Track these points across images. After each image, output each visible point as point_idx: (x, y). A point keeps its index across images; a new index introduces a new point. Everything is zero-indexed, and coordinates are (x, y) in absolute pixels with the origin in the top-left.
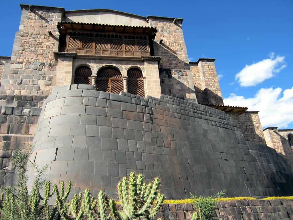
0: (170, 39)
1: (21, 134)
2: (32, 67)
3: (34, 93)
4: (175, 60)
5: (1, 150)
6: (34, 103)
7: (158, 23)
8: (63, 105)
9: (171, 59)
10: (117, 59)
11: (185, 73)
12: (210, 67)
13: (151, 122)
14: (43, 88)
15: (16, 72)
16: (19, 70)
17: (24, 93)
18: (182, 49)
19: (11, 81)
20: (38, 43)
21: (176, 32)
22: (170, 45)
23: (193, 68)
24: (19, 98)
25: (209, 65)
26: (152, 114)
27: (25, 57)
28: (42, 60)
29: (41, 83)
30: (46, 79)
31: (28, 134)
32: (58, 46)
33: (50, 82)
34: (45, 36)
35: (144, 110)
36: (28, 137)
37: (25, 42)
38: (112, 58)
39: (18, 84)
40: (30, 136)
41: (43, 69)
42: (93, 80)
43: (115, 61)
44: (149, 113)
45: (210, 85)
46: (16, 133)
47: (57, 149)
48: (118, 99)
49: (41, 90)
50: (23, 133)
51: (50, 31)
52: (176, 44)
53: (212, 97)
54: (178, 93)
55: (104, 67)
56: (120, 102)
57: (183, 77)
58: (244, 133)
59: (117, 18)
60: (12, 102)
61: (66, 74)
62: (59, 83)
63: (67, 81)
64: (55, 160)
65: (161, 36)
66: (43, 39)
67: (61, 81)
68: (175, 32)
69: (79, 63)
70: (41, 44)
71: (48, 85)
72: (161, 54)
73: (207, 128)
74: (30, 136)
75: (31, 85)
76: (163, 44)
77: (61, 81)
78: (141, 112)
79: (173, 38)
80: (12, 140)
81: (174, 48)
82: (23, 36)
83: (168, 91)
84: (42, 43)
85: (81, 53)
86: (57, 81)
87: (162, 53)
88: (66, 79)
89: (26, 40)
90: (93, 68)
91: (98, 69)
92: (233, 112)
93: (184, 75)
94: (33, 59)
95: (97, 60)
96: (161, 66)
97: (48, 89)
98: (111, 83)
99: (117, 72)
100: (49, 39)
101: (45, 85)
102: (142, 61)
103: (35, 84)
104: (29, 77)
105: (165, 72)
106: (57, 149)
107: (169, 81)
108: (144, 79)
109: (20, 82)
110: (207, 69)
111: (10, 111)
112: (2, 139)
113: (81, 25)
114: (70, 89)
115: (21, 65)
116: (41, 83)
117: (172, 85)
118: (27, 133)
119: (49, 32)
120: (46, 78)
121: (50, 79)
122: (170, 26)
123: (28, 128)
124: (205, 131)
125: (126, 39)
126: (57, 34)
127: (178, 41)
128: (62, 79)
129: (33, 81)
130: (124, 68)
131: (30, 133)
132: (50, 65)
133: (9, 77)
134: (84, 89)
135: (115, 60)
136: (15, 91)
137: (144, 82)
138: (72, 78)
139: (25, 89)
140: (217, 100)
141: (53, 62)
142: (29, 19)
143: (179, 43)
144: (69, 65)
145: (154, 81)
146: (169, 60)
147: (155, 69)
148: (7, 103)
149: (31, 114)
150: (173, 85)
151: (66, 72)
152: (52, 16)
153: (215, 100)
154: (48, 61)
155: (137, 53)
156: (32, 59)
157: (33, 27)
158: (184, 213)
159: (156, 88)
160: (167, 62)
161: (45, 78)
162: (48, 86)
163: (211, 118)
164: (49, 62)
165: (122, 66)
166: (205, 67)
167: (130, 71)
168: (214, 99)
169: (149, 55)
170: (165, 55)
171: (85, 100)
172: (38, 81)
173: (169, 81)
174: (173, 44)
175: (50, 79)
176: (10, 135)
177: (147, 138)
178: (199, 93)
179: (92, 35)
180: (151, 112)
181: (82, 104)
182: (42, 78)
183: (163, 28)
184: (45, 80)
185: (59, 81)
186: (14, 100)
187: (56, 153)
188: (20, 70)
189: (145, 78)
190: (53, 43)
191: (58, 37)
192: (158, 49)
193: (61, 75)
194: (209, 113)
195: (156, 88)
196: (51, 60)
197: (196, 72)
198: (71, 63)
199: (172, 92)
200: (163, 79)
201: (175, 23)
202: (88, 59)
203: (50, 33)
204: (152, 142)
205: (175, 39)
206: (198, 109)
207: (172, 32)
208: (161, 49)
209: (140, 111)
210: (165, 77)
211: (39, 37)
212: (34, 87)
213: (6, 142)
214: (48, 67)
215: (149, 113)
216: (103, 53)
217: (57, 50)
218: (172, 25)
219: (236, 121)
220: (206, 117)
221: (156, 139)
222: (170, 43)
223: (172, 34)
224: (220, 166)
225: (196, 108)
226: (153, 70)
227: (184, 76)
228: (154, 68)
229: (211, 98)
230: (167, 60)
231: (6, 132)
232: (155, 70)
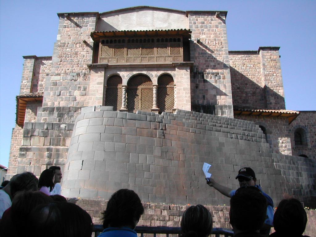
0: (210, 37)
1: (60, 145)
2: (69, 77)
3: (72, 104)
4: (214, 61)
5: (46, 159)
7: (198, 18)
8: (88, 125)
9: (208, 60)
10: (147, 66)
11: (223, 76)
12: (272, 57)
13: (163, 137)
14: (79, 98)
15: (55, 84)
16: (58, 81)
17: (63, 104)
18: (223, 48)
19: (52, 93)
20: (74, 53)
21: (218, 28)
22: (209, 44)
23: (253, 58)
24: (59, 109)
25: (271, 55)
26: (166, 130)
27: (62, 68)
28: (77, 70)
29: (77, 93)
30: (82, 90)
31: (65, 146)
32: (92, 54)
33: (85, 91)
34: (80, 45)
35: (158, 126)
36: (65, 149)
37: (63, 53)
38: (142, 66)
39: (57, 96)
40: (66, 147)
41: (78, 80)
42: (123, 90)
43: (145, 69)
44: (162, 129)
45: (270, 80)
46: (57, 145)
47: (83, 161)
48: (133, 118)
49: (77, 101)
50: (61, 145)
51: (84, 40)
52: (217, 42)
53: (272, 95)
54: (213, 99)
55: (135, 75)
56: (135, 121)
57: (220, 81)
58: (313, 137)
59: (153, 14)
60: (53, 114)
61: (99, 85)
62: (92, 95)
63: (99, 92)
64: (81, 169)
65: (200, 33)
66: (79, 48)
67: (94, 93)
68: (217, 27)
70: (76, 53)
71: (83, 95)
72: (199, 54)
73: (224, 142)
74: (66, 147)
75: (68, 96)
76: (201, 44)
77: (94, 93)
78: (154, 129)
79: (213, 35)
80: (53, 151)
81: (214, 47)
82: (60, 46)
83: (202, 97)
84: (78, 52)
85: (113, 63)
86: (90, 93)
87: (199, 53)
88: (98, 91)
89: (63, 50)
90: (124, 77)
91: (129, 78)
92: (283, 117)
93: (222, 78)
94: (69, 70)
95: (128, 69)
96: (196, 69)
97: (83, 100)
98: (141, 91)
99: (147, 79)
100: (83, 47)
101: (81, 95)
102: (173, 67)
103: (72, 95)
104: (66, 89)
105: (200, 76)
106: (83, 161)
107: (204, 86)
108: (175, 87)
109: (59, 93)
110: (269, 60)
111: (51, 127)
112: (46, 150)
113: (113, 33)
114: (95, 111)
115: (59, 77)
116: (77, 93)
117: (207, 90)
118: (64, 145)
119: (83, 41)
120: (81, 89)
121: (85, 89)
122: (212, 20)
123: (64, 140)
124: (222, 145)
125: (158, 43)
126: (91, 41)
127: (219, 38)
128: (94, 91)
129: (70, 92)
130: (154, 75)
131: (66, 145)
132: (85, 74)
133: (49, 89)
134: (105, 111)
135: (145, 67)
136: (55, 102)
137: (175, 90)
138: (104, 89)
139: (63, 100)
140: (278, 98)
141: (87, 71)
142: (65, 28)
143: (221, 40)
144: (101, 76)
145: (184, 89)
146: (206, 61)
147: (186, 76)
148: (49, 115)
149: (67, 128)
150: (208, 90)
151: (98, 83)
152: (87, 21)
153: (275, 98)
154: (83, 71)
155: (169, 58)
156: (68, 70)
157: (69, 36)
158: (161, 211)
159: (186, 96)
160: (204, 64)
161: (80, 89)
162: (83, 96)
163: (232, 131)
164: (83, 71)
165: (153, 74)
166: (267, 58)
167: (160, 79)
168: (273, 98)
169: (181, 60)
170: (202, 56)
171: (105, 120)
172: (74, 92)
173: (204, 86)
174: (213, 42)
175: (85, 89)
176: (52, 147)
177: (157, 152)
178: (258, 89)
179: (124, 41)
180: (164, 128)
181: (102, 124)
182: (78, 88)
183: (204, 23)
184: (80, 90)
185: (92, 93)
186: (55, 112)
187: (82, 164)
188: (59, 82)
189: (175, 85)
190: (88, 51)
191: (92, 44)
192: (195, 50)
193: (93, 87)
194: (231, 125)
195: (186, 96)
196: (85, 70)
197: (256, 63)
198: (103, 72)
199: (206, 98)
200: (197, 84)
201: (217, 17)
202: (119, 68)
203: (85, 42)
204: (161, 155)
205: (215, 36)
206: (218, 122)
207: (213, 27)
208: (198, 50)
209: (154, 128)
210: (199, 81)
211: (74, 46)
213: (49, 152)
214: (83, 77)
215: (162, 129)
216: (134, 60)
217: (90, 63)
218: (213, 19)
219: (285, 127)
220: (226, 130)
221: (164, 153)
222: (210, 42)
223: (213, 31)
224: (230, 178)
225: (215, 121)
226: (184, 76)
227: (221, 80)
228: (185, 75)
229: (270, 96)
230: (204, 62)
231: (48, 144)
232: (186, 77)
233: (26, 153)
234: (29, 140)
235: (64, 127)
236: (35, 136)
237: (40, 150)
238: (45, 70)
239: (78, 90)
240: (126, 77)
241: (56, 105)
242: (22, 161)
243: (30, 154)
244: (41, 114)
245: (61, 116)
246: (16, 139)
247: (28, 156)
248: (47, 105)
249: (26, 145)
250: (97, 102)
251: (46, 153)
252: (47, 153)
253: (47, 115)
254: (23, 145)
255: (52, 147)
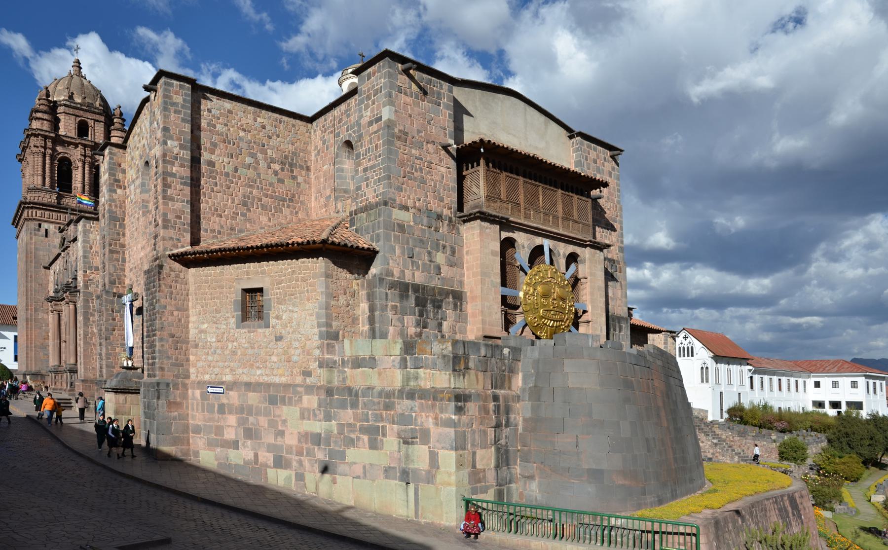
6: (438, 301)
17: (419, 278)
24: (416, 288)
28: (435, 206)
29: (440, 258)
30: (448, 253)
31: (511, 390)
49: (442, 275)
60: (407, 296)
69: (505, 235)
75: (428, 262)
103: (433, 260)
129: (429, 253)
175: (453, 253)
182: (441, 248)
212: (432, 267)
214: (448, 225)
233: (465, 404)
234: (462, 377)
235: (508, 354)
236: (470, 369)
237: (483, 398)
238: (218, 126)
239: (443, 253)
240: (526, 249)
241: (408, 279)
242: (459, 420)
243: (472, 407)
244: (387, 294)
245: (421, 303)
246: (172, 293)
247: (468, 411)
248: (393, 275)
249: (458, 388)
250: (493, 290)
251: (492, 405)
252: (493, 403)
253: (398, 299)
254: (454, 388)
255: (497, 391)
